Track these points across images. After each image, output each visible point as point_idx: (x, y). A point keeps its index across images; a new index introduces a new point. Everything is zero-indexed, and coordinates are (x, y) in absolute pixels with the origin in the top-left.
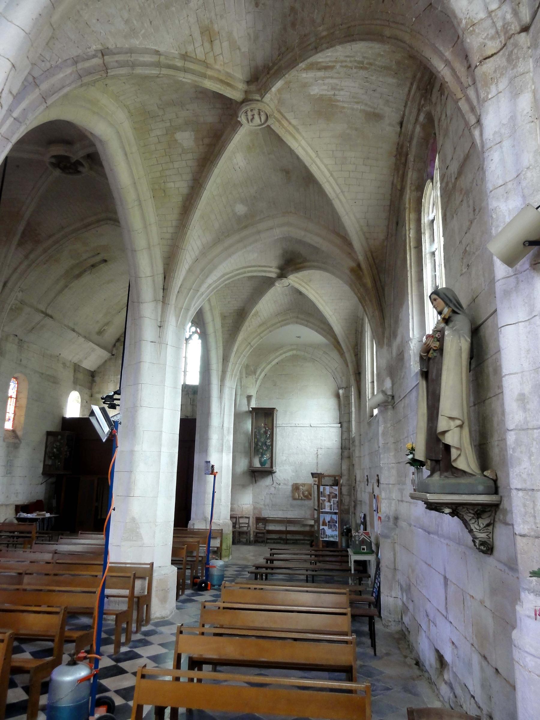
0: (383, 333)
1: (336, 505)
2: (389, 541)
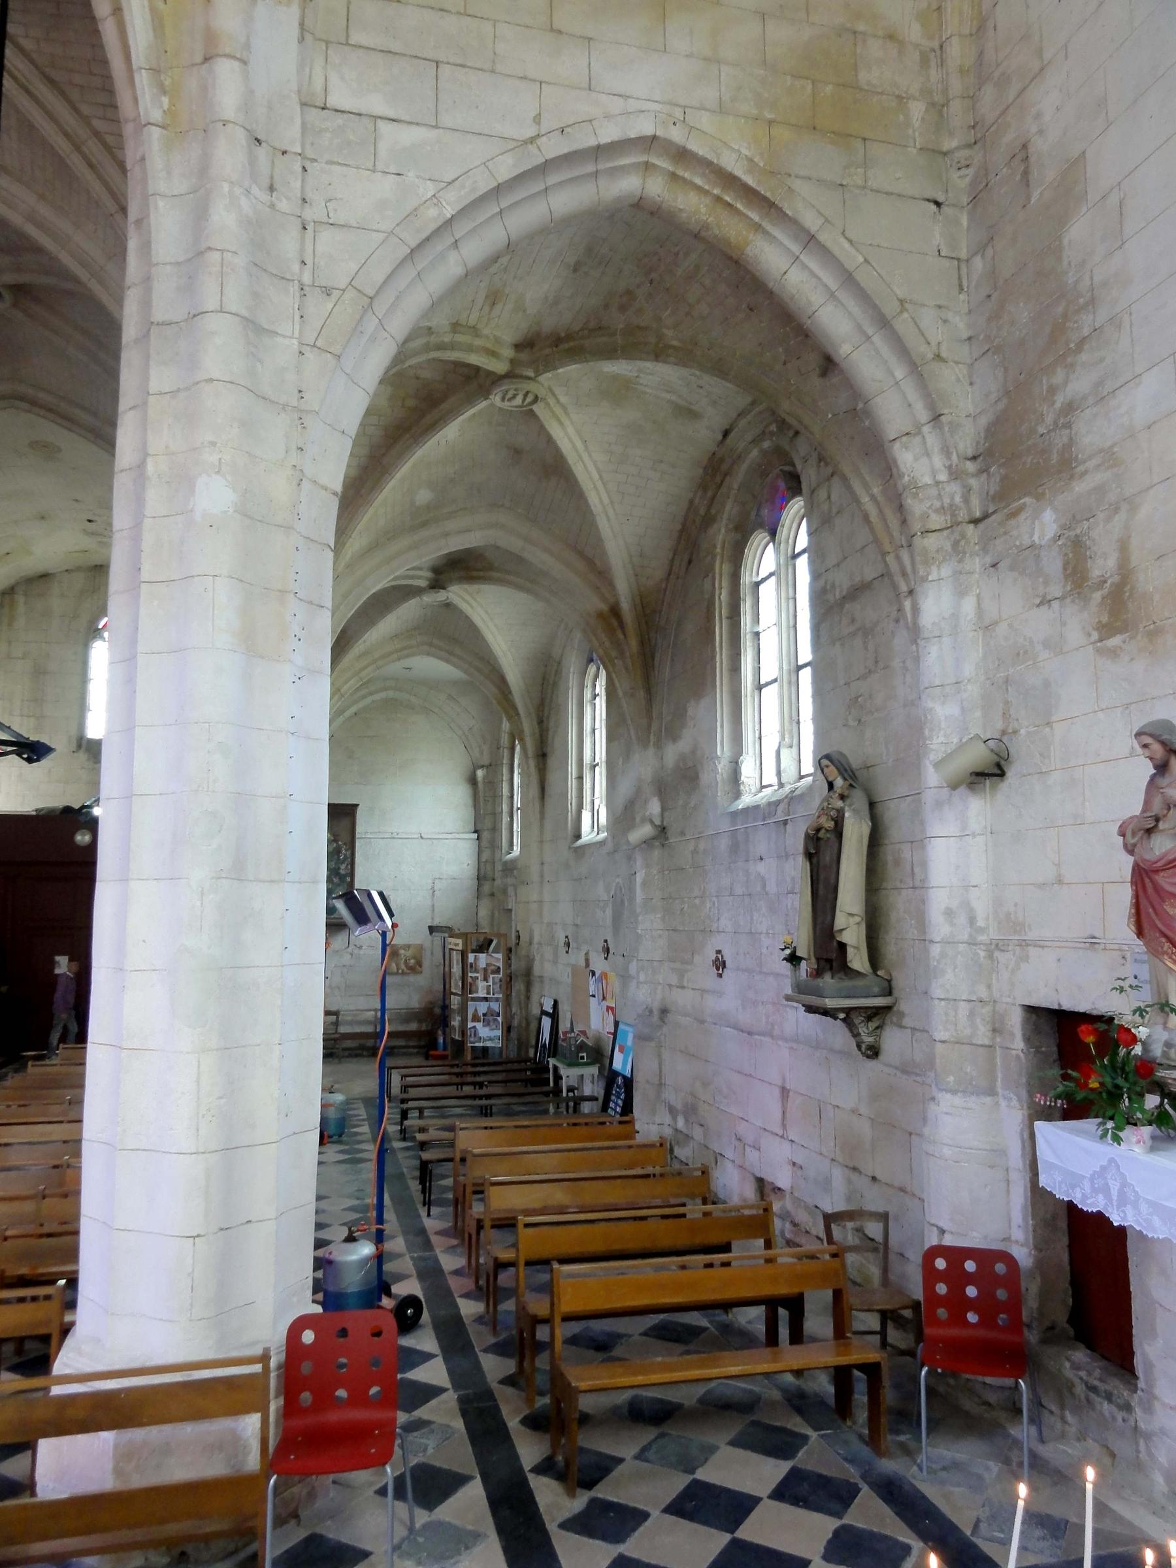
0: (649, 726)
2: (653, 1044)
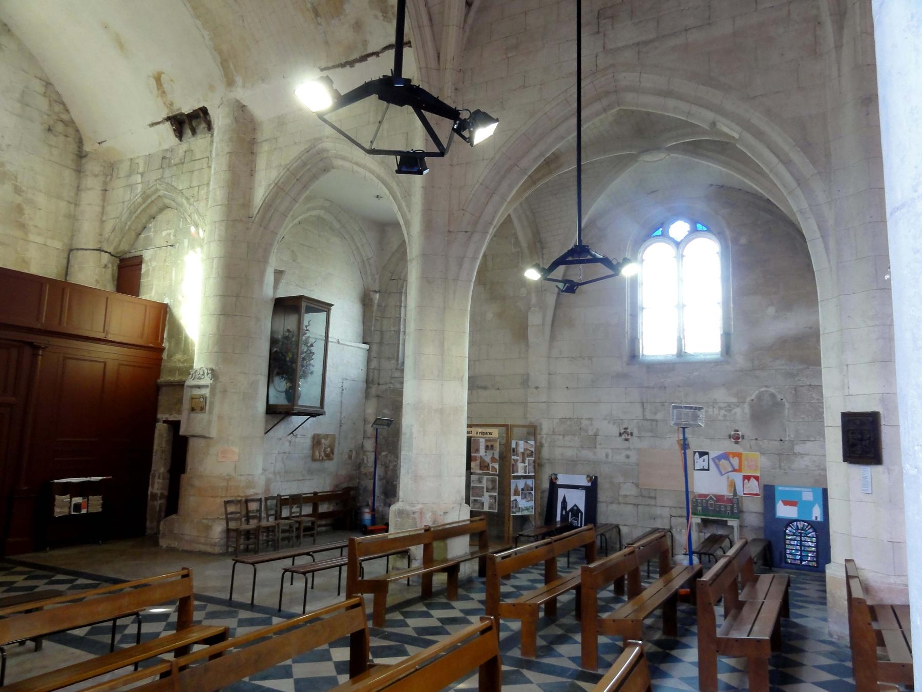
1: (531, 467)
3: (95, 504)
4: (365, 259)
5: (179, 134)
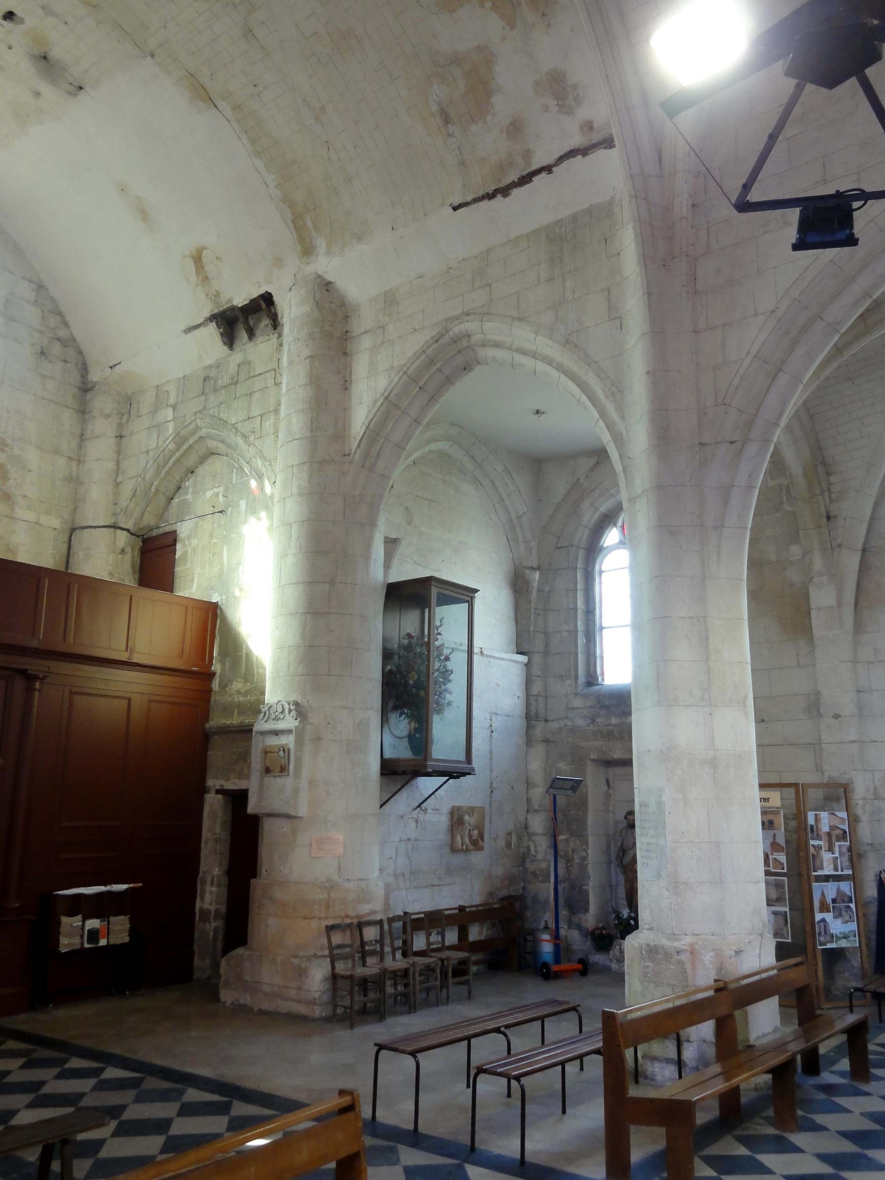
1: (846, 858)
3: (118, 930)
4: (514, 516)
5: (230, 339)
